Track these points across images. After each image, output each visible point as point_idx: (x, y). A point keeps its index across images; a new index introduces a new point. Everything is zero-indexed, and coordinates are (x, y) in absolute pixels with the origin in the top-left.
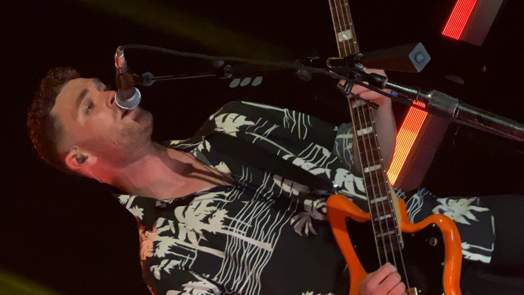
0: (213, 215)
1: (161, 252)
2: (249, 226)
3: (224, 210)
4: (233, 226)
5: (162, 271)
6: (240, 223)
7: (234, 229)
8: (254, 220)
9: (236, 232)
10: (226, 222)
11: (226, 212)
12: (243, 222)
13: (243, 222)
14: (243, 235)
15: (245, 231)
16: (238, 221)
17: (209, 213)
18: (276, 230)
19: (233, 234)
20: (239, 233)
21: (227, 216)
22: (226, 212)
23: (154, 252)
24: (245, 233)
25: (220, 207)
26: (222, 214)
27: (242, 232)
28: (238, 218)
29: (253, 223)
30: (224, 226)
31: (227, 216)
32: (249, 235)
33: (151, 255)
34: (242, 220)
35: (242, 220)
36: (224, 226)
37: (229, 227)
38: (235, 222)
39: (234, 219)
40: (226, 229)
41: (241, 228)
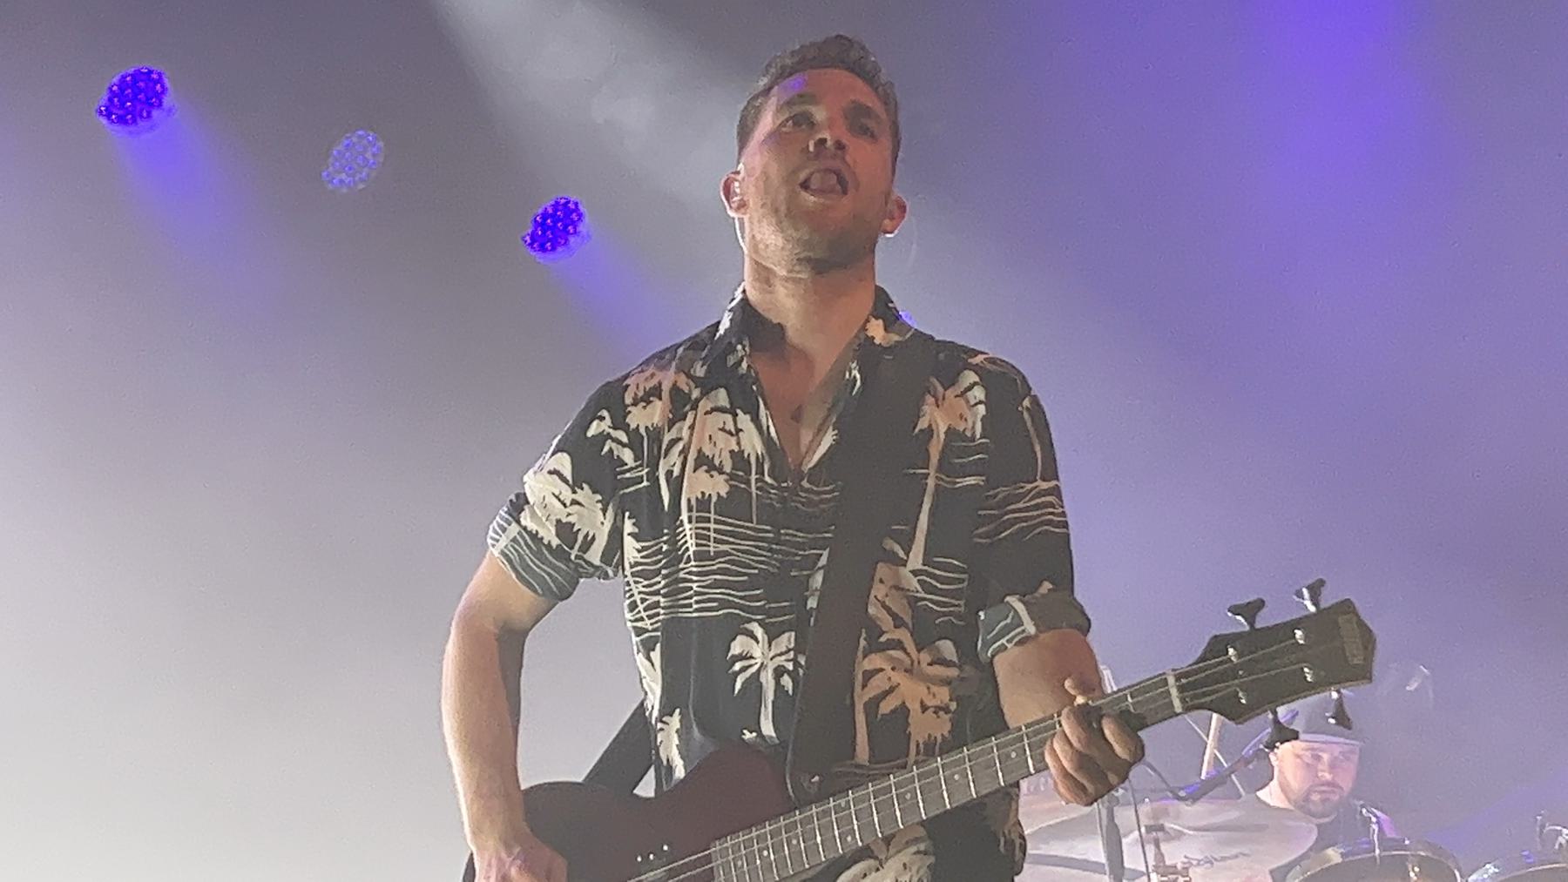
0: (714, 473)
1: (639, 418)
3: (727, 489)
5: (603, 437)
7: (694, 525)
8: (727, 553)
10: (703, 503)
11: (723, 494)
12: (712, 535)
13: (712, 535)
16: (712, 526)
17: (717, 462)
18: (724, 604)
19: (687, 526)
21: (714, 499)
22: (723, 494)
23: (635, 404)
25: (732, 477)
26: (717, 486)
28: (716, 522)
29: (718, 554)
30: (693, 502)
31: (714, 499)
33: (628, 401)
34: (716, 531)
35: (716, 531)
36: (693, 502)
37: (694, 514)
38: (709, 521)
39: (712, 516)
40: (690, 509)
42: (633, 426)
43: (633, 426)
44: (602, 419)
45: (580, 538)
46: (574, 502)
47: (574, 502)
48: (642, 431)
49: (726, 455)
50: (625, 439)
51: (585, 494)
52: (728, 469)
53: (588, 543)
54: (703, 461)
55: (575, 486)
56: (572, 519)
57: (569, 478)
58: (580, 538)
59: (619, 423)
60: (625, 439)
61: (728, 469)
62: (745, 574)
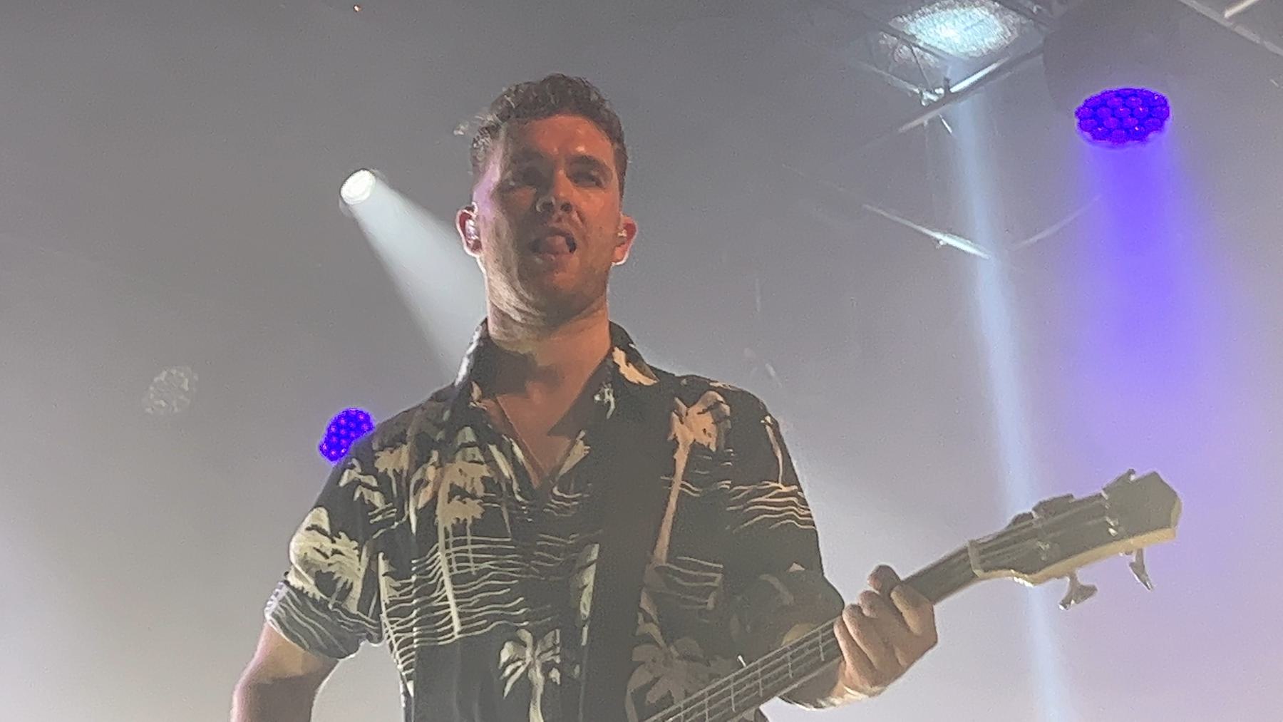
1: (386, 462)
2: (473, 570)
4: (456, 544)
6: (466, 551)
9: (448, 555)
12: (471, 556)
13: (471, 556)
14: (451, 570)
15: (459, 568)
16: (469, 547)
20: (450, 562)
23: (382, 449)
24: (456, 572)
27: (454, 565)
28: (474, 542)
29: (482, 573)
30: (450, 529)
31: (470, 522)
32: (454, 580)
33: (375, 447)
34: (474, 551)
35: (474, 551)
36: (450, 529)
38: (465, 543)
39: (469, 538)
40: (447, 536)
41: (458, 560)
42: (381, 470)
43: (381, 470)
44: (352, 467)
45: (340, 585)
46: (335, 552)
47: (335, 552)
48: (390, 473)
49: (478, 481)
50: (375, 484)
51: (344, 543)
52: (480, 493)
53: (347, 590)
54: (457, 492)
55: (333, 536)
56: (332, 569)
57: (326, 527)
58: (340, 585)
59: (369, 469)
60: (375, 484)
61: (480, 493)
62: (508, 586)
